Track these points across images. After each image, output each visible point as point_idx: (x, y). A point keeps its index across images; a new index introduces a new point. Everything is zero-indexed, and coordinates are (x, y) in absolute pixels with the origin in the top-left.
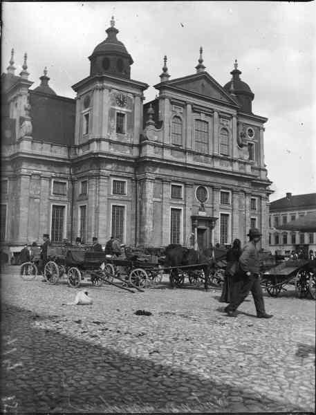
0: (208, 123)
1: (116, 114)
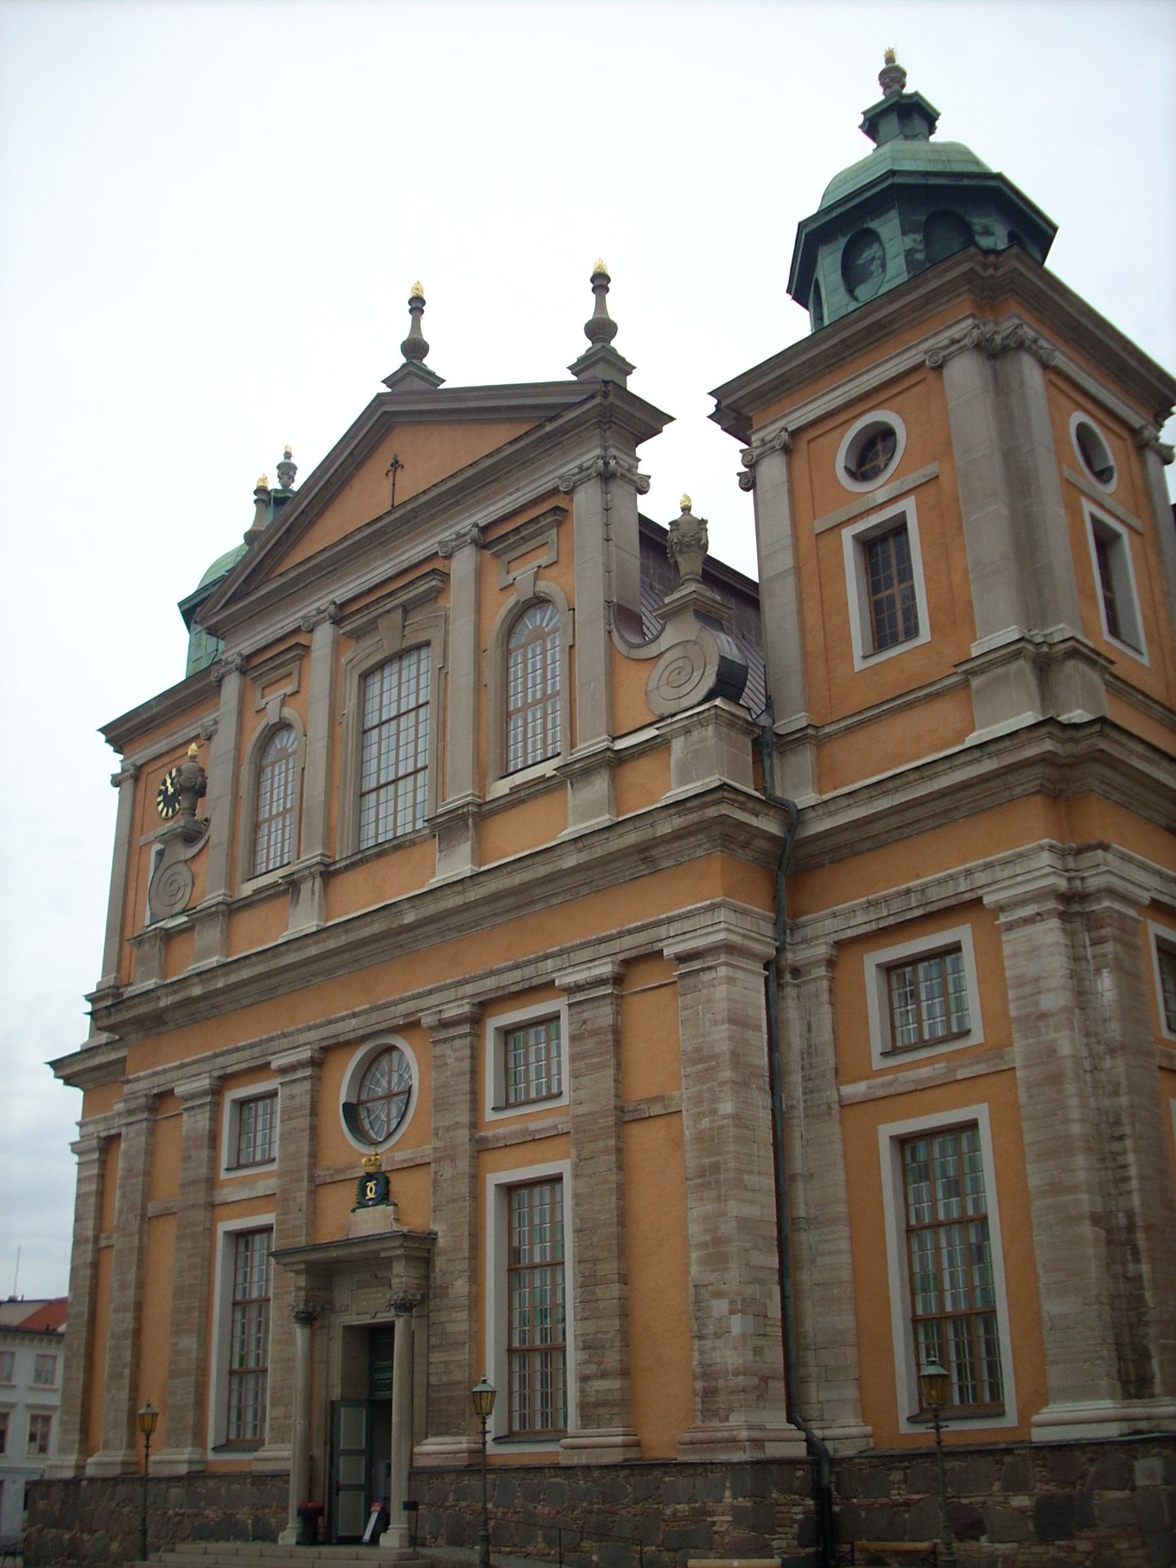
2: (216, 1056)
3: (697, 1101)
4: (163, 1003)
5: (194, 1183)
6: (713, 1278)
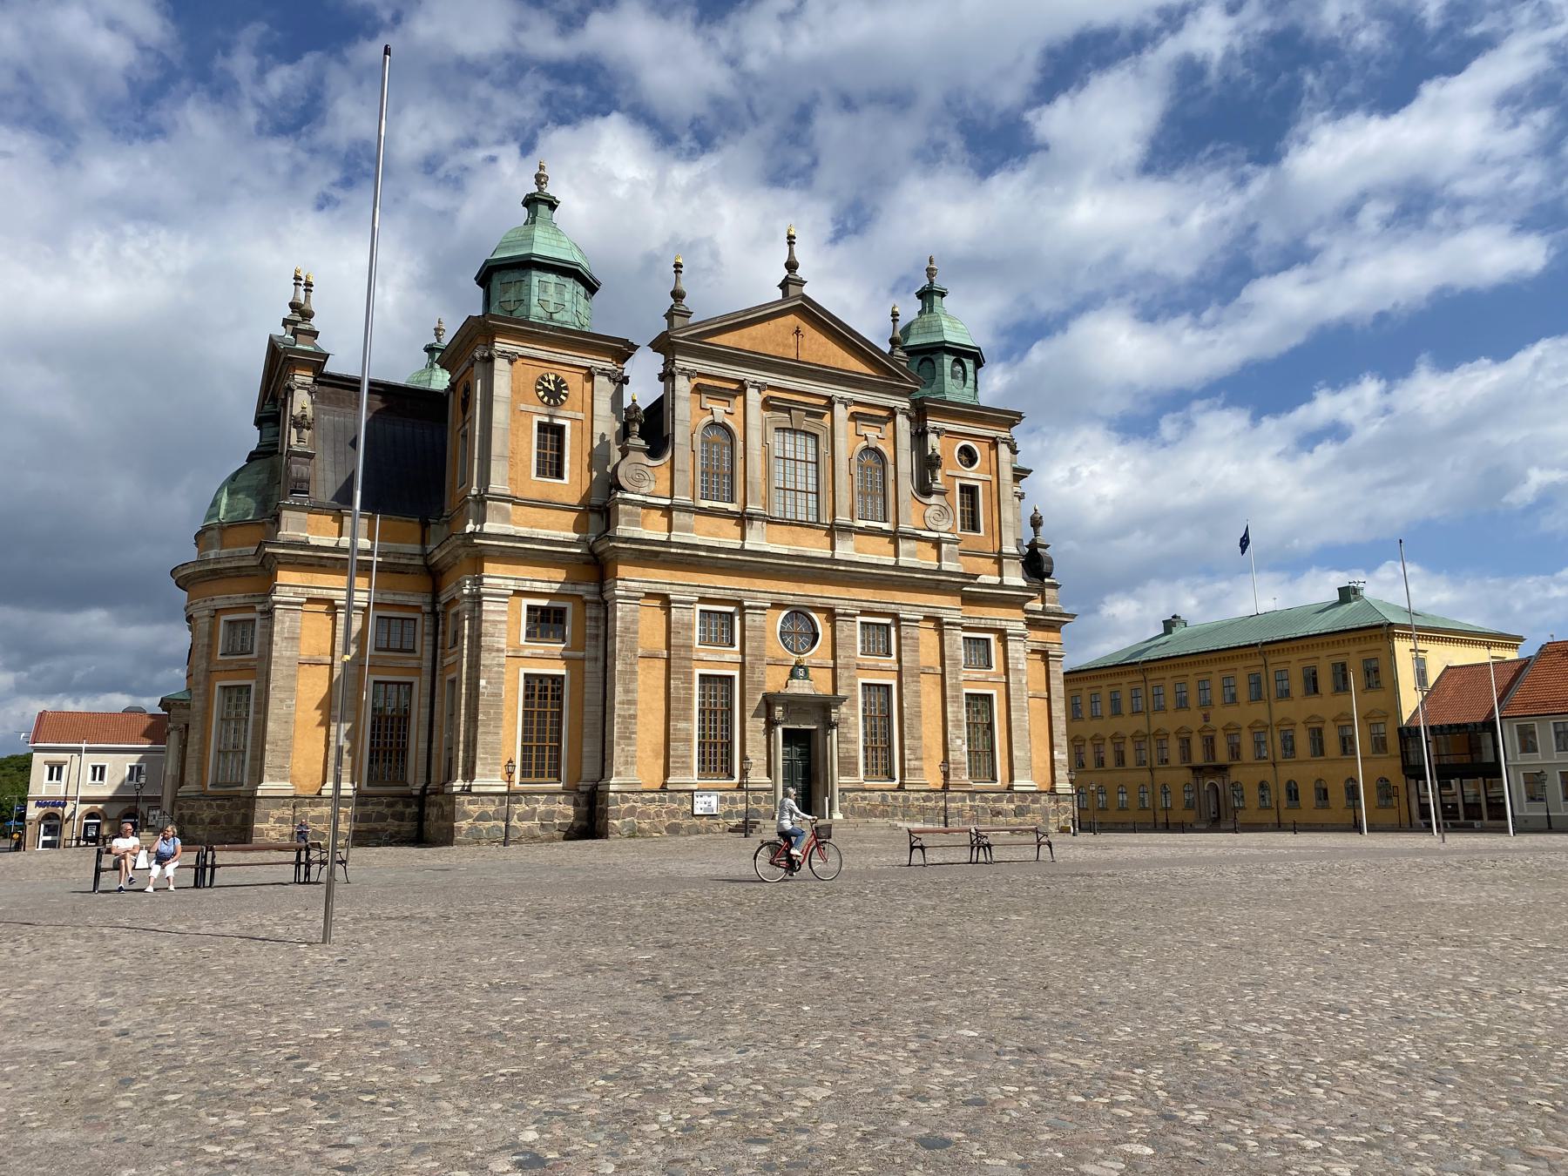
0: (816, 436)
1: (535, 427)
2: (699, 586)
3: (951, 673)
4: (673, 550)
5: (683, 646)
6: (957, 732)
